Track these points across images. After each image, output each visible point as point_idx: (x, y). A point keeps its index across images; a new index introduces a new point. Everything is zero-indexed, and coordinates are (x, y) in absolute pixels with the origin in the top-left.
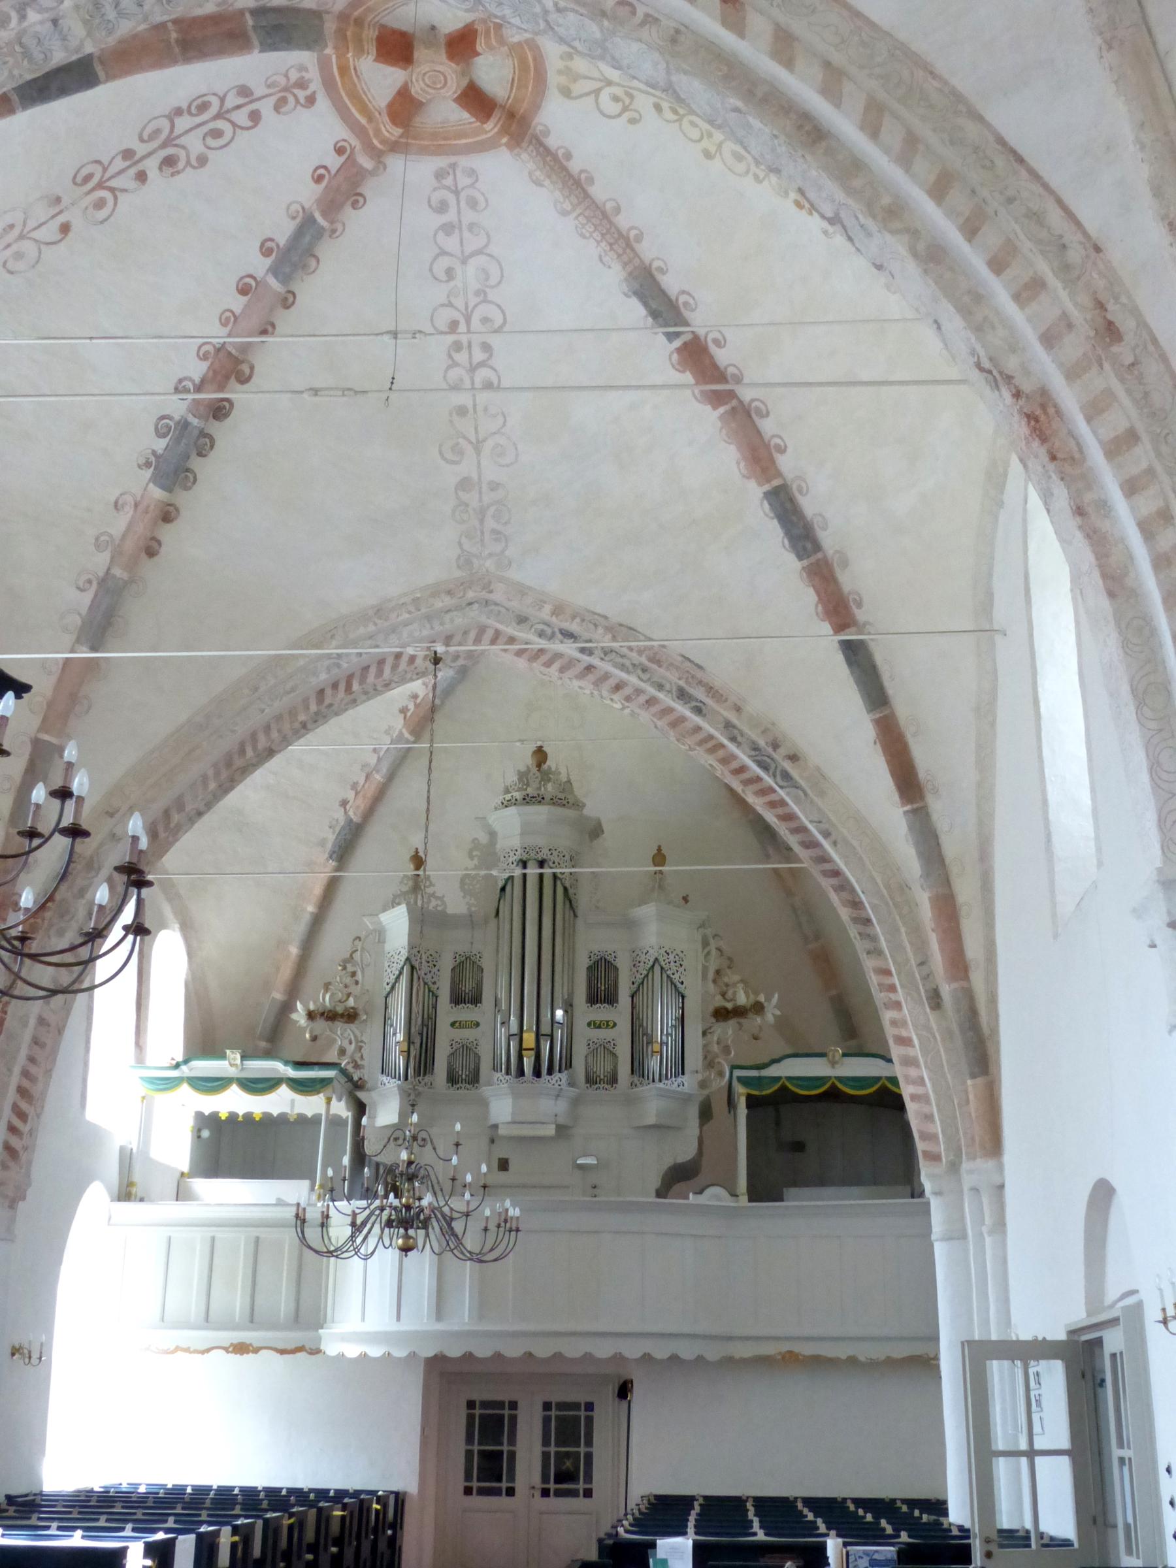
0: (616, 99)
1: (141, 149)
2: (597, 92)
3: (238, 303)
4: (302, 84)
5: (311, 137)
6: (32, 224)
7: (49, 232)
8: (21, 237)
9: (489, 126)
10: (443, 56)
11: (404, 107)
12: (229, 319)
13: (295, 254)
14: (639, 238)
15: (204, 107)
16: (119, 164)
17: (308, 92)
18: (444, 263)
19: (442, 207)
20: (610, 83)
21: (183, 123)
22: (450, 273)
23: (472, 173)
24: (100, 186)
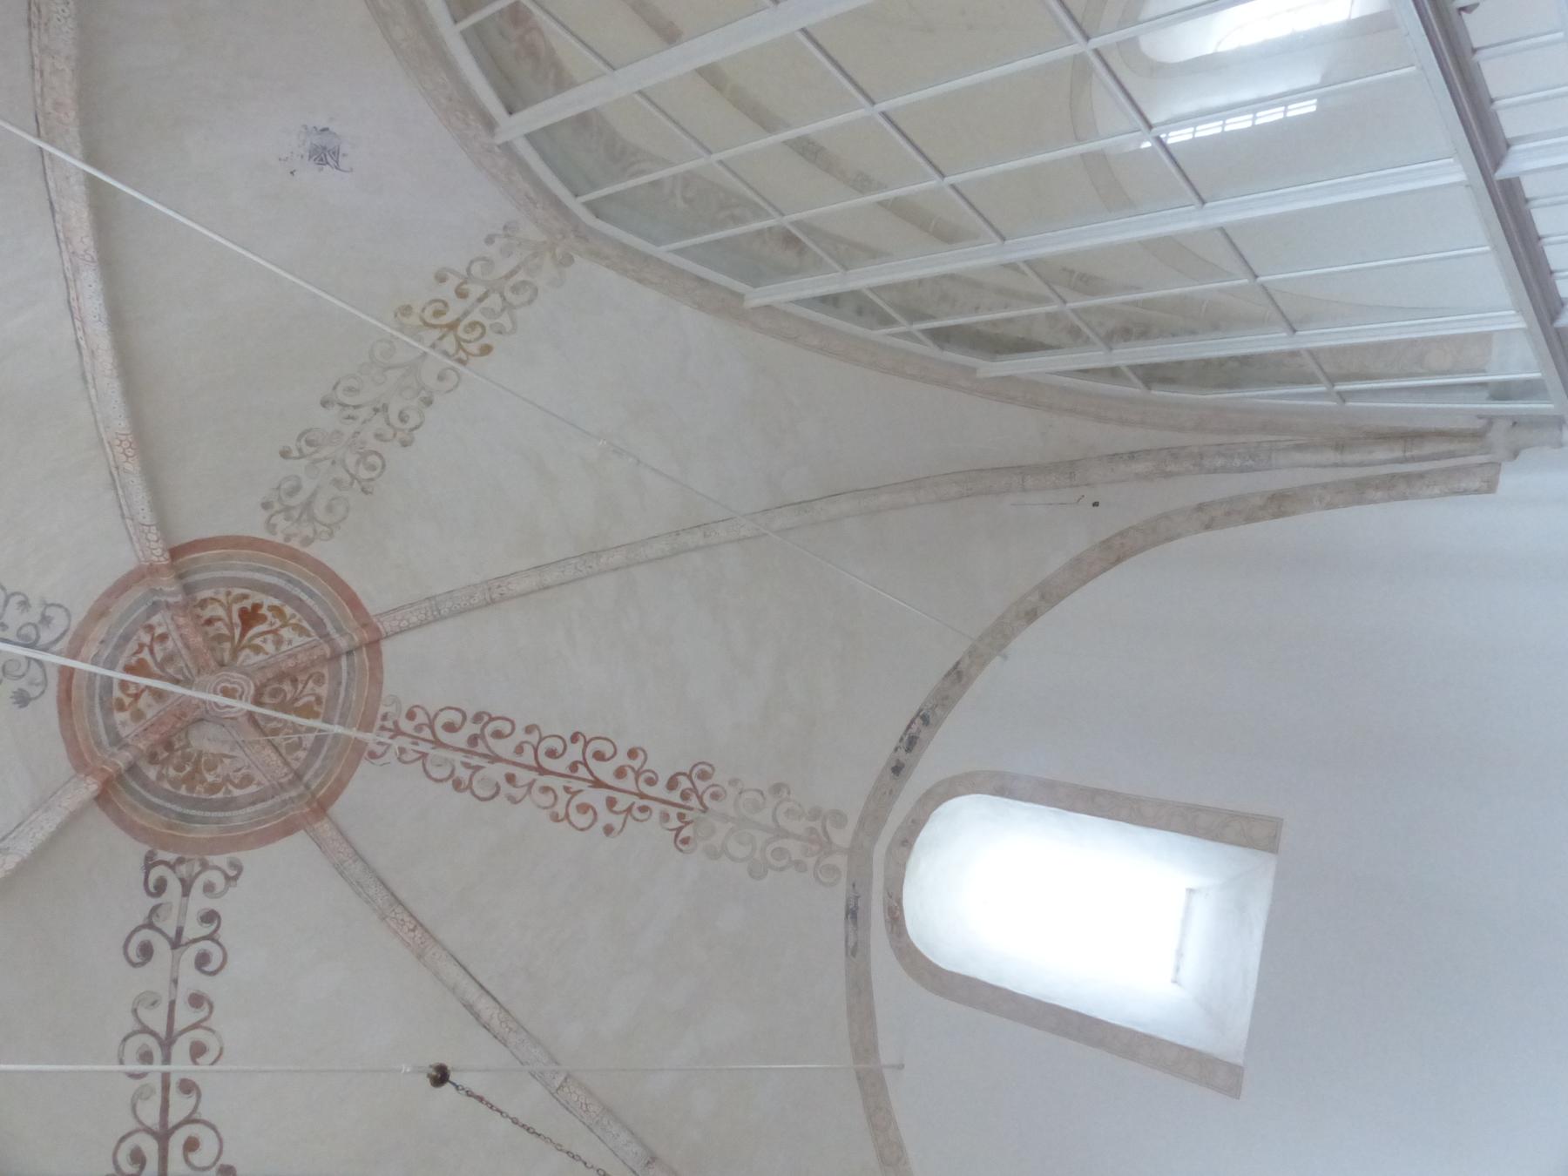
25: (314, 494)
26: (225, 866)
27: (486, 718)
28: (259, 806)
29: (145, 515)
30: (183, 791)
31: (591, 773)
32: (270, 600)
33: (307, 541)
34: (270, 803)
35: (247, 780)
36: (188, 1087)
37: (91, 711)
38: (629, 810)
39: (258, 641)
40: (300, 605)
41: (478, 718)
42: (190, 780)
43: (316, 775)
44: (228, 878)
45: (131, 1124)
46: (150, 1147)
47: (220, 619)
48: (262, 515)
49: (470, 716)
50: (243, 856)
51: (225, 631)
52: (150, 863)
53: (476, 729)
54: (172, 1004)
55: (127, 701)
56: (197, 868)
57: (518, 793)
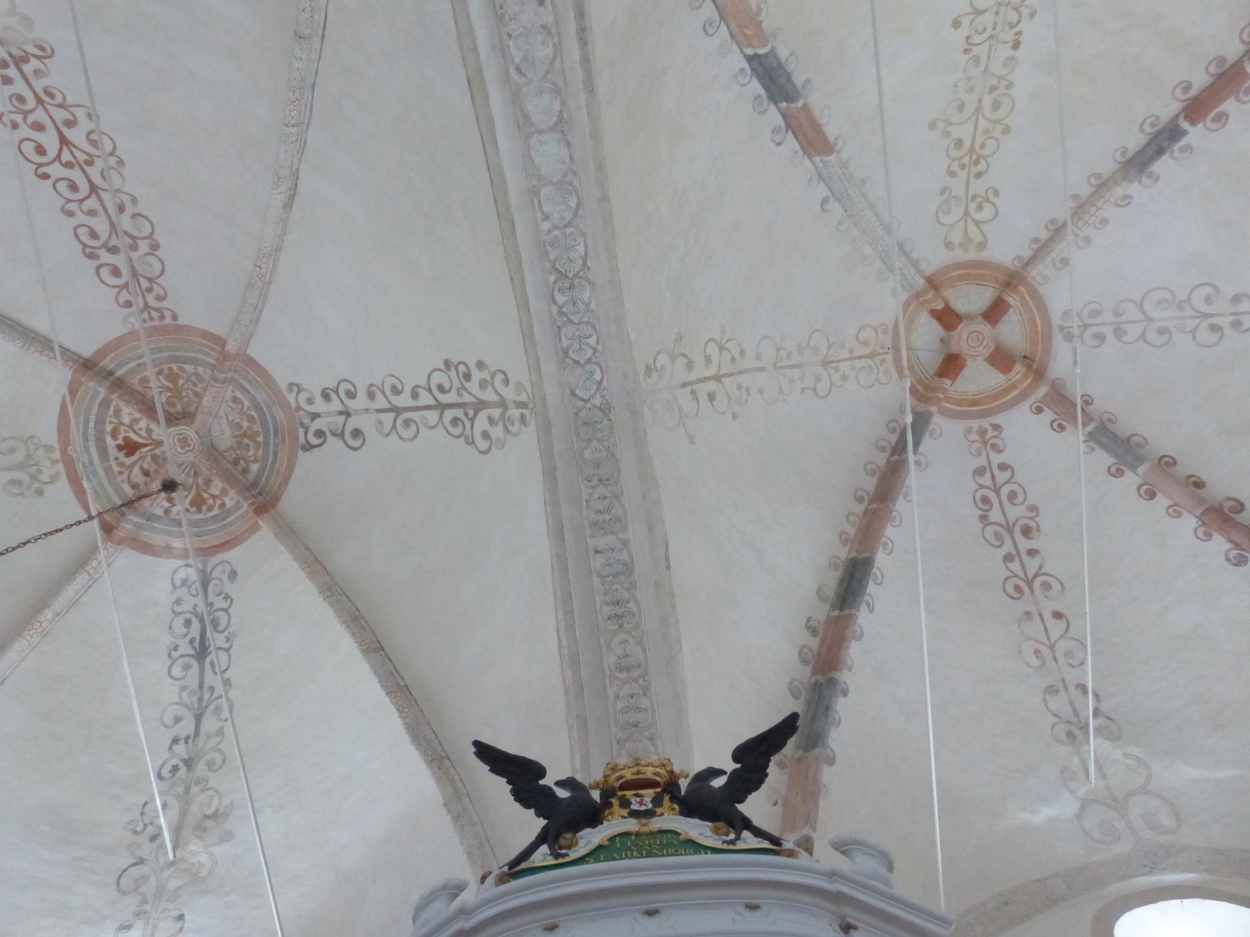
0: (980, 208)
1: (1008, 547)
2: (977, 223)
3: (1162, 502)
4: (983, 432)
5: (1026, 432)
6: (1043, 638)
7: (1056, 628)
8: (1052, 647)
9: (1010, 300)
10: (955, 334)
11: (1001, 359)
12: (1175, 511)
13: (1121, 448)
14: (1097, 176)
15: (985, 500)
16: (1015, 566)
17: (990, 429)
18: (1152, 336)
19: (1101, 338)
20: (967, 214)
21: (995, 515)
22: (1161, 332)
23: (1067, 314)
24: (1030, 584)
25: (9, 469)
26: (294, 395)
27: (88, 250)
28: (247, 387)
29: (82, 578)
30: (260, 439)
31: (61, 150)
32: (110, 443)
33: (48, 448)
34: (241, 381)
35: (235, 400)
36: (415, 396)
37: (230, 524)
38: (61, 106)
39: (143, 433)
40: (100, 423)
41: (92, 256)
42: (252, 436)
43: (208, 355)
44: (299, 391)
45: (440, 428)
46: (449, 414)
47: (142, 468)
48: (50, 490)
49: (97, 263)
50: (283, 386)
51: (149, 459)
52: (308, 447)
53: (103, 254)
54: (378, 411)
55: (218, 502)
56: (302, 413)
57: (127, 200)
